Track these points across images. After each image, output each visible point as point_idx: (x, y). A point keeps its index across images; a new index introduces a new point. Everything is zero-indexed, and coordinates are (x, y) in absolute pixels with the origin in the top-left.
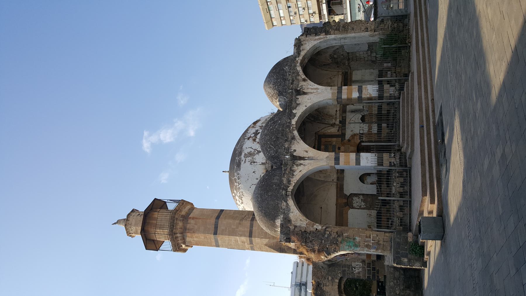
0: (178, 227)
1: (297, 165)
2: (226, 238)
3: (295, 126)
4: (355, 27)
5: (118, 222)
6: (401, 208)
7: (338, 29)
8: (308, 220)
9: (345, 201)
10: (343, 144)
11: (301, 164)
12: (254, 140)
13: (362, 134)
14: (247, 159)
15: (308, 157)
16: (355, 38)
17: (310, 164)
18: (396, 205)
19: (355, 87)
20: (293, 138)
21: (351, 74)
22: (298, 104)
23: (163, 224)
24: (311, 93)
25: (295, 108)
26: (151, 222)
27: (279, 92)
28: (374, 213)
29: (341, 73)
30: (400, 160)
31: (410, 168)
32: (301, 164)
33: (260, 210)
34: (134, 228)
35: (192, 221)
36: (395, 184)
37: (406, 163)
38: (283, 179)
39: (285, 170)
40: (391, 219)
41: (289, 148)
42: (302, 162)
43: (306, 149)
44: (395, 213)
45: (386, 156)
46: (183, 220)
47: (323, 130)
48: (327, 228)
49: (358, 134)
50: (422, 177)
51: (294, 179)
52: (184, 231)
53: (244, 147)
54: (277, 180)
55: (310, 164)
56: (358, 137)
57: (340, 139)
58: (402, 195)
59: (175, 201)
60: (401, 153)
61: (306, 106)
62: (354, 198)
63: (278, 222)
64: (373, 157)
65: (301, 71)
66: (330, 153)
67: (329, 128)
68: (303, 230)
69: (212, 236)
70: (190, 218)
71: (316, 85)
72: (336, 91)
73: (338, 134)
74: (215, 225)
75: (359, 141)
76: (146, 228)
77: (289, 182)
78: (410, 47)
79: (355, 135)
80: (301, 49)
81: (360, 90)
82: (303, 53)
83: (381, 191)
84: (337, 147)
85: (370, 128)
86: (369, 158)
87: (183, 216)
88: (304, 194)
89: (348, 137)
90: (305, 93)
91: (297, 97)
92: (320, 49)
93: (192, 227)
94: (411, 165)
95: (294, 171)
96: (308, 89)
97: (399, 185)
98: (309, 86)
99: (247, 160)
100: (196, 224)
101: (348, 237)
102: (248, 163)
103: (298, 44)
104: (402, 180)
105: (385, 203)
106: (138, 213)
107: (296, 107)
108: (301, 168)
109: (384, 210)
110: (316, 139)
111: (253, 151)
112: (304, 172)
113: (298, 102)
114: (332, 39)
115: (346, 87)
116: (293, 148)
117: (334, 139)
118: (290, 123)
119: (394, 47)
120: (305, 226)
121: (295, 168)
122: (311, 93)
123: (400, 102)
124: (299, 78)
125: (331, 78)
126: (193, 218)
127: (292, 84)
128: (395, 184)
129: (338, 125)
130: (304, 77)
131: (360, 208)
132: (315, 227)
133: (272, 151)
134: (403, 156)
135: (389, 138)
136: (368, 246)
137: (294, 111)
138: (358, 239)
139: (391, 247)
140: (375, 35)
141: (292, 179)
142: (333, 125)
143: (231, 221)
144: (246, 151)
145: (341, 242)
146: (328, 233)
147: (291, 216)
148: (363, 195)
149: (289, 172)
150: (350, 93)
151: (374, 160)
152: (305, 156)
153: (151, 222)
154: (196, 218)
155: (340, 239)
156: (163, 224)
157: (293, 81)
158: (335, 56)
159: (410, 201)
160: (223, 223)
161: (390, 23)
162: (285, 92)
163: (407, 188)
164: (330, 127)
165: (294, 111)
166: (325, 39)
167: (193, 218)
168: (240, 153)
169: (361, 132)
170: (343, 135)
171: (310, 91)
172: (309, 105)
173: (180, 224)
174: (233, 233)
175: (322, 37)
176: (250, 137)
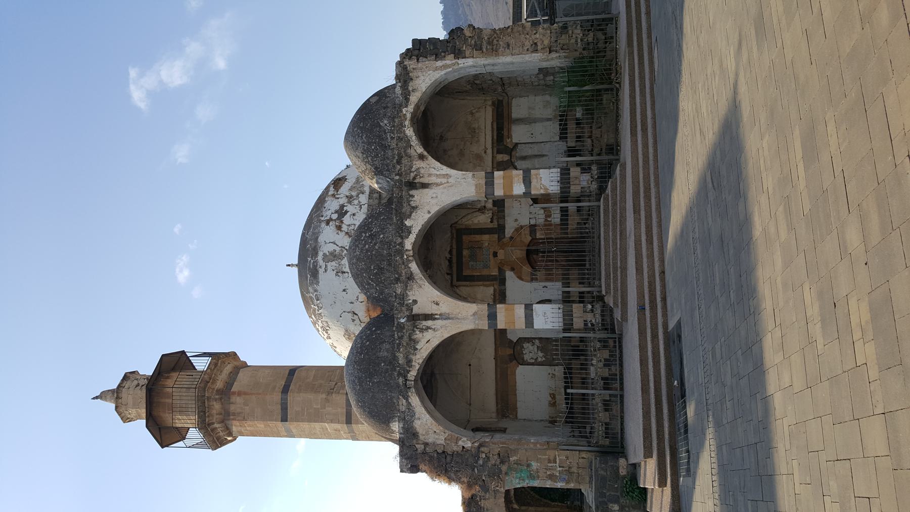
0: (214, 412)
1: (422, 330)
2: (305, 425)
3: (411, 253)
4: (512, 42)
5: (102, 396)
6: (607, 406)
7: (478, 48)
8: (448, 433)
9: (509, 351)
10: (503, 246)
11: (428, 328)
12: (339, 228)
14: (329, 264)
15: (440, 315)
16: (513, 63)
17: (446, 327)
18: (598, 402)
19: (517, 175)
20: (411, 277)
21: (509, 105)
22: (414, 208)
23: (187, 399)
24: (437, 185)
25: (409, 216)
26: (163, 400)
27: (376, 168)
28: (559, 371)
29: (490, 103)
30: (603, 320)
31: (621, 334)
32: (428, 328)
33: (361, 407)
34: (133, 412)
35: (238, 400)
36: (594, 362)
37: (613, 324)
38: (397, 354)
39: (401, 338)
40: (589, 423)
41: (403, 297)
42: (429, 323)
43: (436, 299)
44: (596, 416)
45: (577, 308)
46: (221, 399)
48: (481, 445)
50: (644, 417)
51: (418, 356)
52: (226, 417)
53: (321, 239)
54: (387, 351)
55: (446, 327)
56: (527, 232)
58: (607, 383)
59: (205, 354)
60: (603, 306)
61: (429, 212)
62: (526, 345)
63: (396, 426)
64: (554, 315)
65: (414, 138)
66: (480, 306)
67: (475, 214)
68: (440, 451)
69: (280, 424)
70: (234, 393)
71: (445, 167)
72: (483, 182)
73: (491, 226)
74: (282, 404)
75: (529, 238)
76: (155, 413)
77: (409, 362)
78: (618, 90)
79: (522, 227)
80: (410, 89)
81: (527, 181)
82: (414, 98)
83: (571, 378)
84: (492, 251)
85: (548, 215)
86: (549, 315)
87: (219, 392)
88: (435, 379)
90: (425, 186)
91: (411, 192)
92: (446, 82)
93: (239, 410)
94: (622, 331)
95: (416, 342)
96: (430, 175)
97: (601, 365)
98: (432, 169)
99: (329, 267)
100: (246, 404)
101: (517, 463)
102: (331, 274)
103: (404, 75)
104: (606, 354)
105: (578, 350)
106: (136, 382)
107: (411, 213)
108: (428, 335)
109: (575, 364)
111: (338, 249)
112: (435, 342)
113: (413, 204)
114: (470, 64)
115: (501, 173)
116: (412, 295)
118: (402, 244)
119: (587, 91)
120: (442, 442)
121: (418, 335)
122: (437, 185)
123: (599, 206)
124: (411, 152)
125: (472, 114)
126: (239, 394)
127: (399, 162)
128: (594, 362)
130: (420, 150)
131: (536, 363)
132: (460, 443)
133: (373, 291)
134: (607, 311)
135: (581, 233)
136: (551, 477)
137: (408, 223)
138: (535, 465)
139: (591, 477)
140: (552, 59)
141: (414, 358)
143: (311, 396)
144: (326, 249)
145: (506, 474)
146: (484, 456)
147: (417, 424)
148: (540, 339)
149: (407, 344)
150: (509, 185)
151: (557, 320)
152: (434, 312)
153: (163, 400)
154: (245, 394)
155: (504, 468)
156: (187, 399)
157: (400, 157)
158: (477, 82)
159: (622, 396)
160: (296, 399)
161: (578, 31)
162: (388, 170)
163: (615, 369)
165: (408, 223)
166: (456, 67)
167: (239, 394)
168: (315, 254)
169: (533, 222)
170: (501, 229)
171: (433, 180)
172: (434, 209)
173: (217, 406)
174: (316, 417)
175: (448, 62)
176: (331, 219)
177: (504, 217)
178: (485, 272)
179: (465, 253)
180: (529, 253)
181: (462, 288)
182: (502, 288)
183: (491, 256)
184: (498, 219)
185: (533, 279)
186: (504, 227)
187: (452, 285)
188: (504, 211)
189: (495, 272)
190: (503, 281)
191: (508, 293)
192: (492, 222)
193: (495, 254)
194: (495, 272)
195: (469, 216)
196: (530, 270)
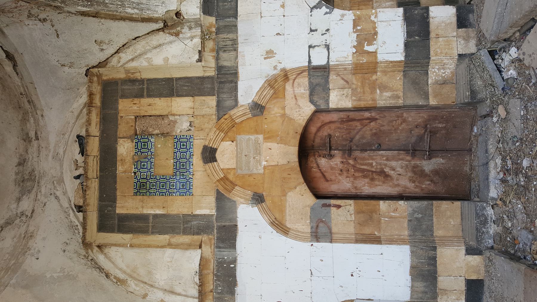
10: (230, 130)
13: (325, 70)
47: (125, 56)
49: (300, 72)
56: (301, 86)
57: (212, 101)
73: (197, 72)
75: (308, 109)
79: (285, 75)
85: (366, 35)
89: (249, 89)
110: (90, 104)
117: (182, 105)
129: (198, 23)
142: (172, 23)
164: (163, 37)
169: (319, 59)
170: (224, 81)
177: (234, 46)
178: (178, 206)
179: (125, 148)
180: (306, 150)
181: (112, 252)
182: (226, 254)
183: (197, 160)
184: (218, 51)
185: (320, 233)
186: (235, 74)
187: (86, 245)
188: (233, 28)
189: (206, 207)
190: (227, 235)
191: (243, 273)
192: (200, 60)
193: (209, 155)
194: (206, 207)
195: (140, 46)
196: (310, 199)
